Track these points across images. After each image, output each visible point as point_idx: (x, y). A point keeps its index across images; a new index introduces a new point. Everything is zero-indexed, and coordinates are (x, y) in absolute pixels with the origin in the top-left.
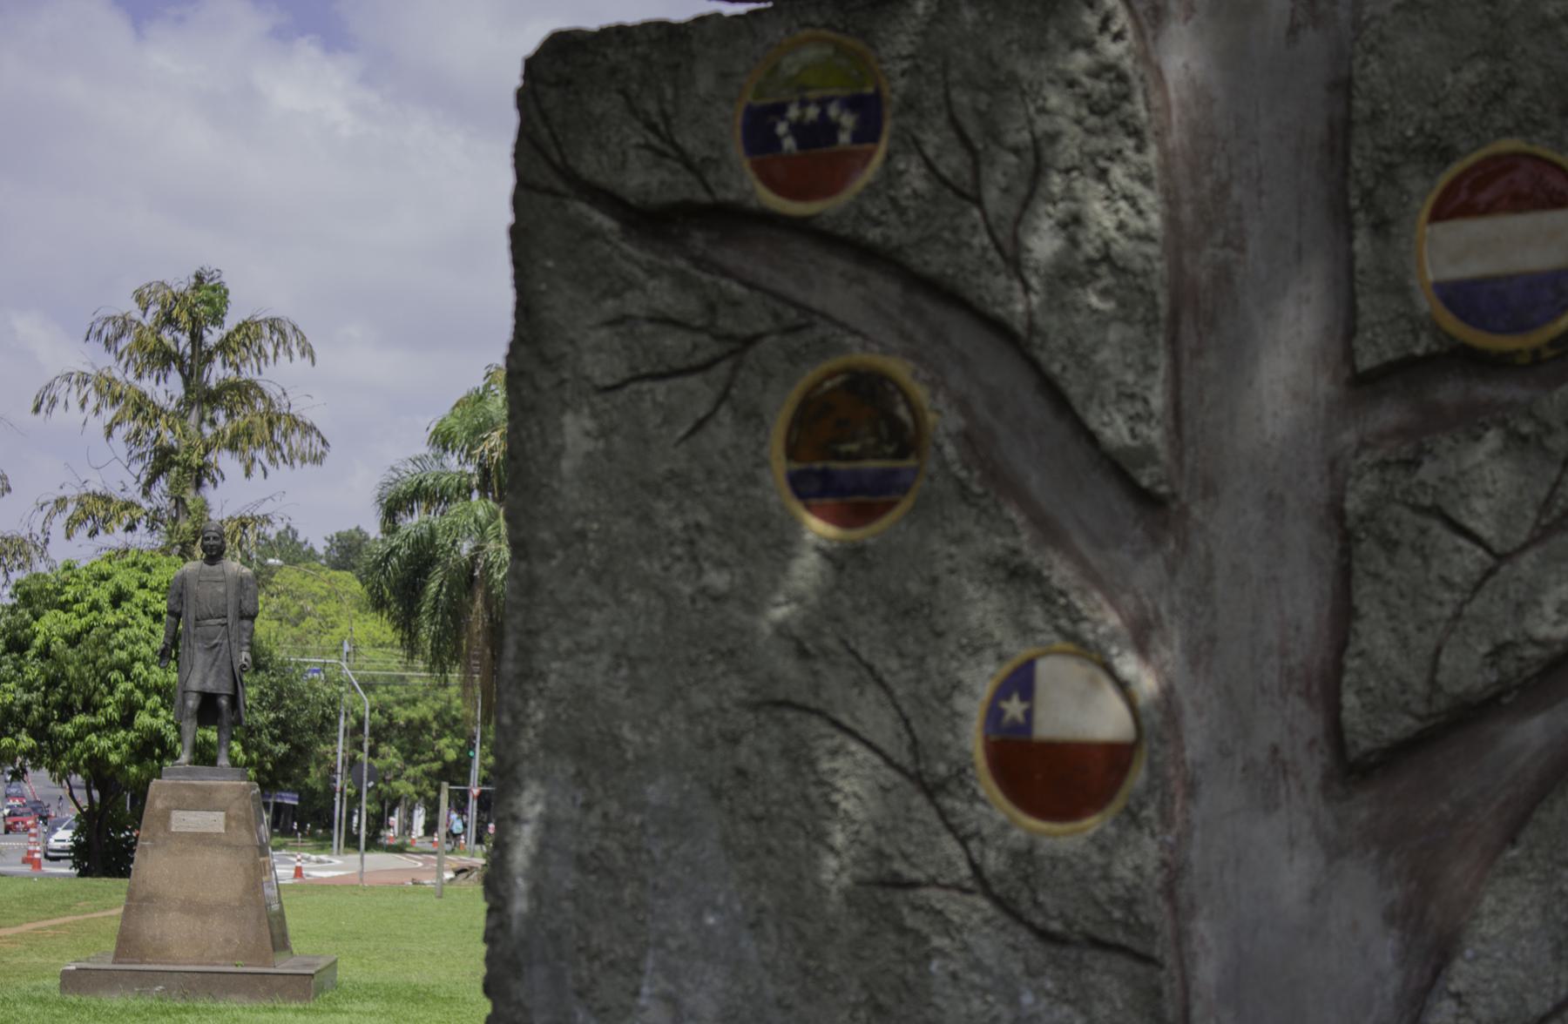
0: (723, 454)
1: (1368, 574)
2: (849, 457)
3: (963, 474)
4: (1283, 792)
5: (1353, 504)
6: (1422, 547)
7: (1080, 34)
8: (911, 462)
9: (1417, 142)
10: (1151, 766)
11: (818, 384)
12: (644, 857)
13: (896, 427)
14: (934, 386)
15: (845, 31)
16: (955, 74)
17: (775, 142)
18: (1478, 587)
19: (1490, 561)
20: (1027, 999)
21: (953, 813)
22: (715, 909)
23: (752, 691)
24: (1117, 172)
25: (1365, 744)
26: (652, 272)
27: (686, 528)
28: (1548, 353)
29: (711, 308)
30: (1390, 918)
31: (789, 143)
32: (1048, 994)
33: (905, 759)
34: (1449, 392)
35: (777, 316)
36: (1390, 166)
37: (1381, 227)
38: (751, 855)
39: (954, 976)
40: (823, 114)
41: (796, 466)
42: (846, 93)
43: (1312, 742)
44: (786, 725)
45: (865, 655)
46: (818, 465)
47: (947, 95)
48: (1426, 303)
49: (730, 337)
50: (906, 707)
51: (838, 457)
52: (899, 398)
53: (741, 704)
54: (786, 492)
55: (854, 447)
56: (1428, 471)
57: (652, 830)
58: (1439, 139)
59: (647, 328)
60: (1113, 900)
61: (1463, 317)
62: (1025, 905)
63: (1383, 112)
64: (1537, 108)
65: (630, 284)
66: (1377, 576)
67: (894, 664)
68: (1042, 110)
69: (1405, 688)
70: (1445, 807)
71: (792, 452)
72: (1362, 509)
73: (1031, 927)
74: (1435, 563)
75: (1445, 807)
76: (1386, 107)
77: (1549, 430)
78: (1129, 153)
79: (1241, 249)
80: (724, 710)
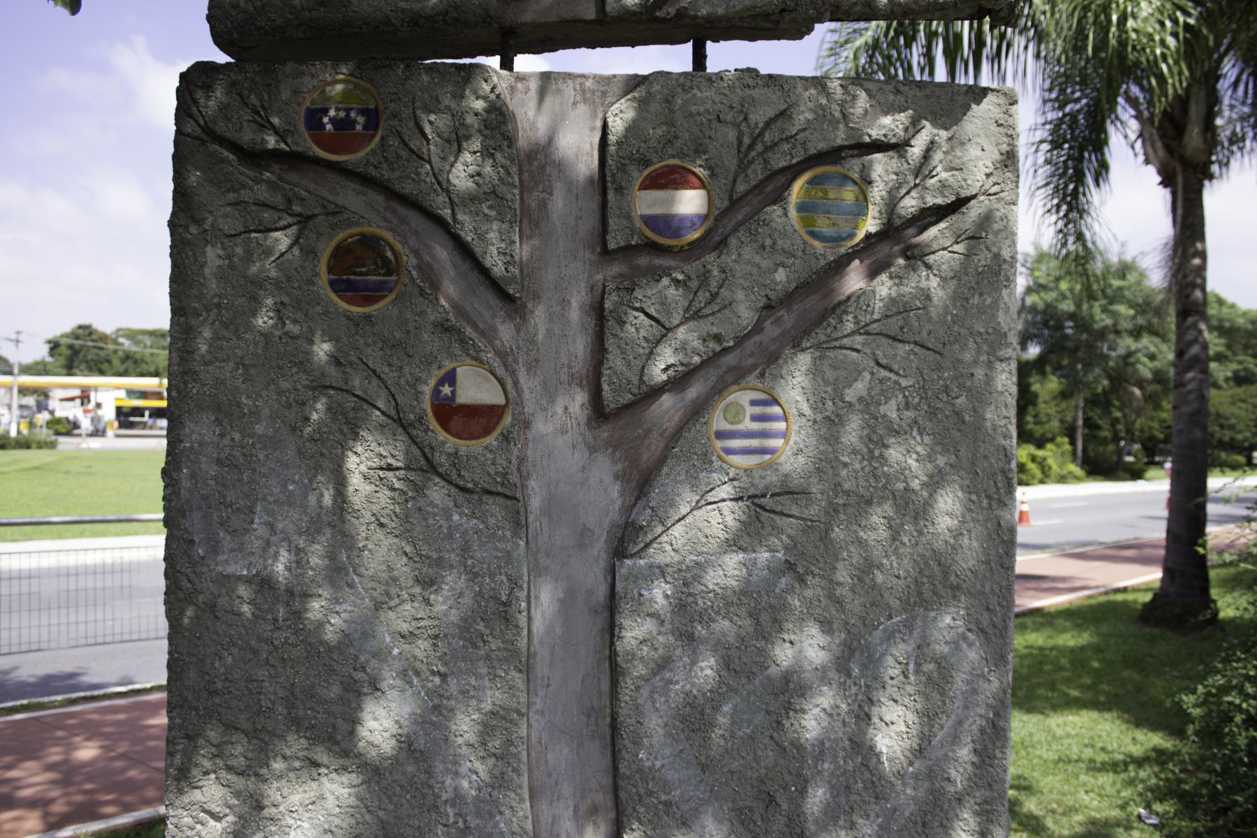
0: (296, 270)
2: (361, 274)
3: (422, 284)
5: (608, 305)
7: (481, 93)
8: (394, 278)
9: (636, 156)
10: (513, 415)
11: (346, 239)
12: (254, 458)
13: (386, 261)
14: (404, 244)
15: (361, 78)
16: (418, 104)
17: (323, 126)
20: (456, 517)
21: (417, 436)
22: (294, 482)
23: (312, 381)
24: (498, 156)
25: (612, 406)
26: (256, 182)
27: (275, 303)
28: (687, 248)
29: (289, 201)
30: (616, 477)
31: (329, 127)
32: (466, 515)
33: (393, 413)
34: (643, 260)
35: (324, 207)
36: (624, 165)
37: (619, 190)
38: (312, 457)
39: (420, 509)
40: (348, 115)
41: (332, 277)
42: (360, 107)
43: (583, 405)
45: (371, 365)
46: (345, 277)
47: (414, 113)
48: (639, 224)
49: (299, 215)
50: (392, 389)
51: (355, 274)
52: (387, 248)
53: (307, 387)
54: (328, 289)
55: (364, 270)
56: (638, 293)
57: (258, 446)
59: (254, 208)
60: (497, 473)
61: (653, 230)
62: (454, 476)
65: (244, 187)
66: (616, 336)
67: (387, 370)
68: (462, 124)
69: (629, 382)
70: (640, 431)
71: (330, 271)
72: (611, 307)
73: (457, 486)
77: (690, 278)
78: (505, 148)
79: (551, 194)
80: (296, 389)
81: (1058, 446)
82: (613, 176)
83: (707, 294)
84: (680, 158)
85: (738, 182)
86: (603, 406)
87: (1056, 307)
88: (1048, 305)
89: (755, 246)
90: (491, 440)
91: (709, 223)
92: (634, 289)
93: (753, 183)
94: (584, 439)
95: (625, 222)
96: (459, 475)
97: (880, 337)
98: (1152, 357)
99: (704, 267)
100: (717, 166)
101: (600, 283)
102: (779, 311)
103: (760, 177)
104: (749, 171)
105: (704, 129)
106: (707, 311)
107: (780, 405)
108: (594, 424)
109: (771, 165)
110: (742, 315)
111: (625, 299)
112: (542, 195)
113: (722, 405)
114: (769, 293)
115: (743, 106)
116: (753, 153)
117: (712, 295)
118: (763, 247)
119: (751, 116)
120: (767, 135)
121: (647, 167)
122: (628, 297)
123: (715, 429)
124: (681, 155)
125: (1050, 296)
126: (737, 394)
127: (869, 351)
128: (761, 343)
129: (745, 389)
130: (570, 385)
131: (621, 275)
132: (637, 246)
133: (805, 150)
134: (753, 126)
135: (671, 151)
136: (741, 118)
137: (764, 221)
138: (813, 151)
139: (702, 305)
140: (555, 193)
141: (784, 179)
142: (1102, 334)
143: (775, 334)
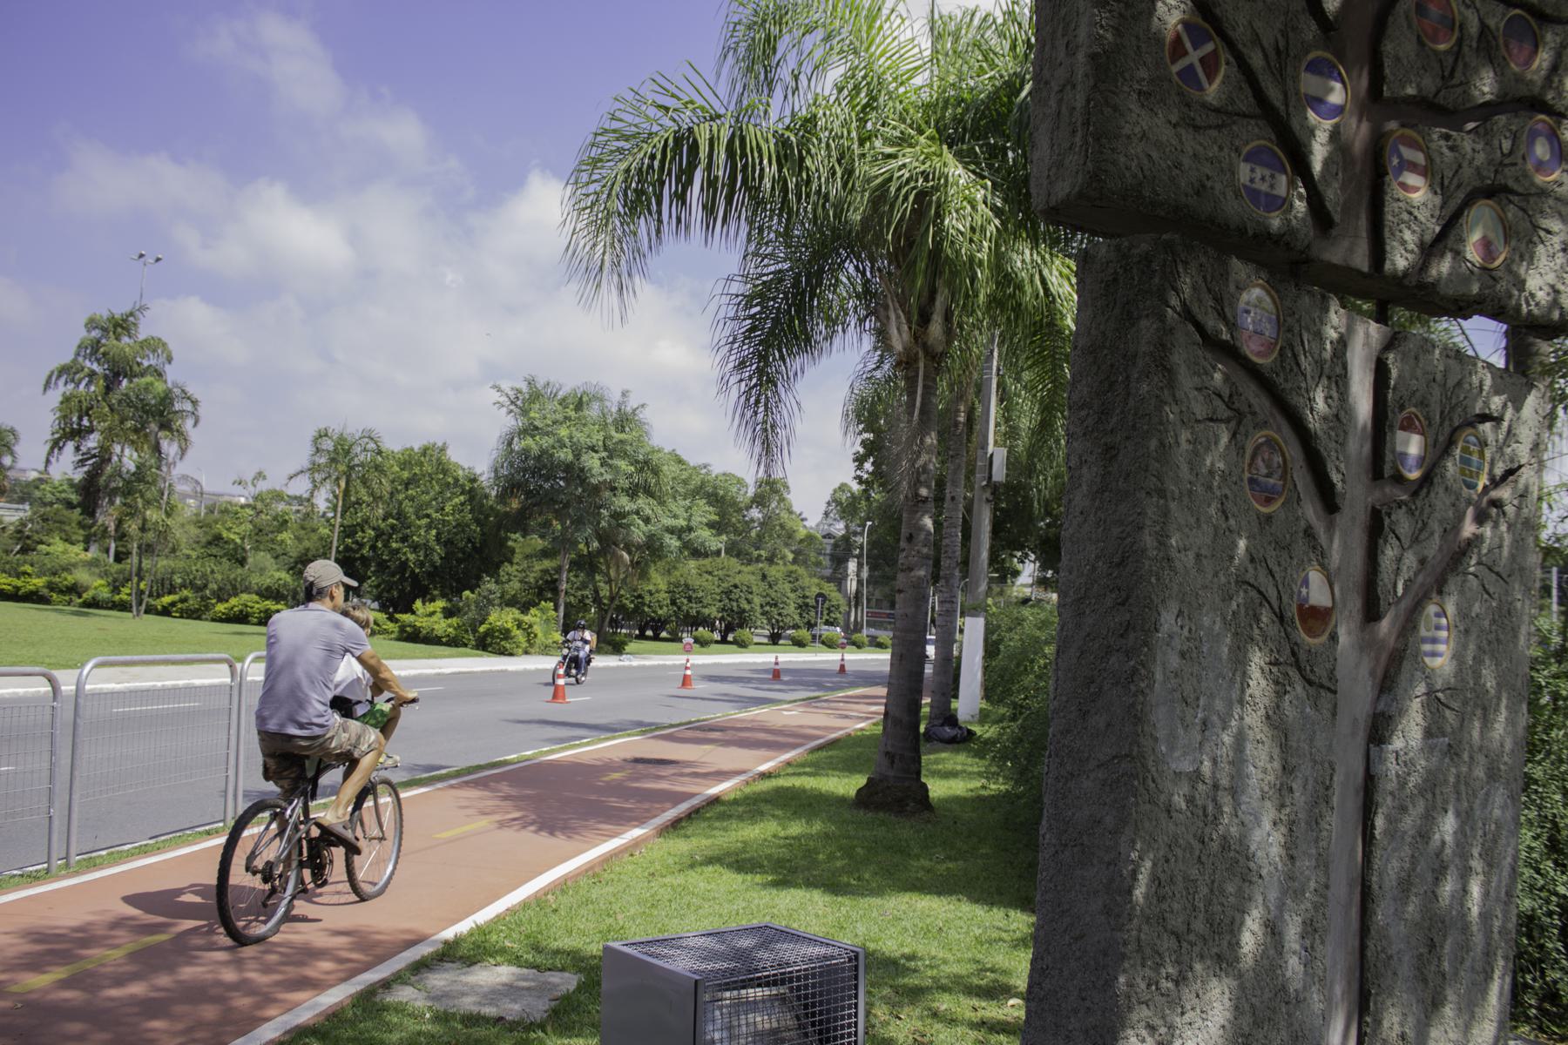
44: (1246, 592)
81: (543, 611)
87: (552, 455)
88: (543, 452)
90: (1324, 638)
96: (1312, 671)
98: (647, 520)
125: (546, 442)
142: (596, 490)
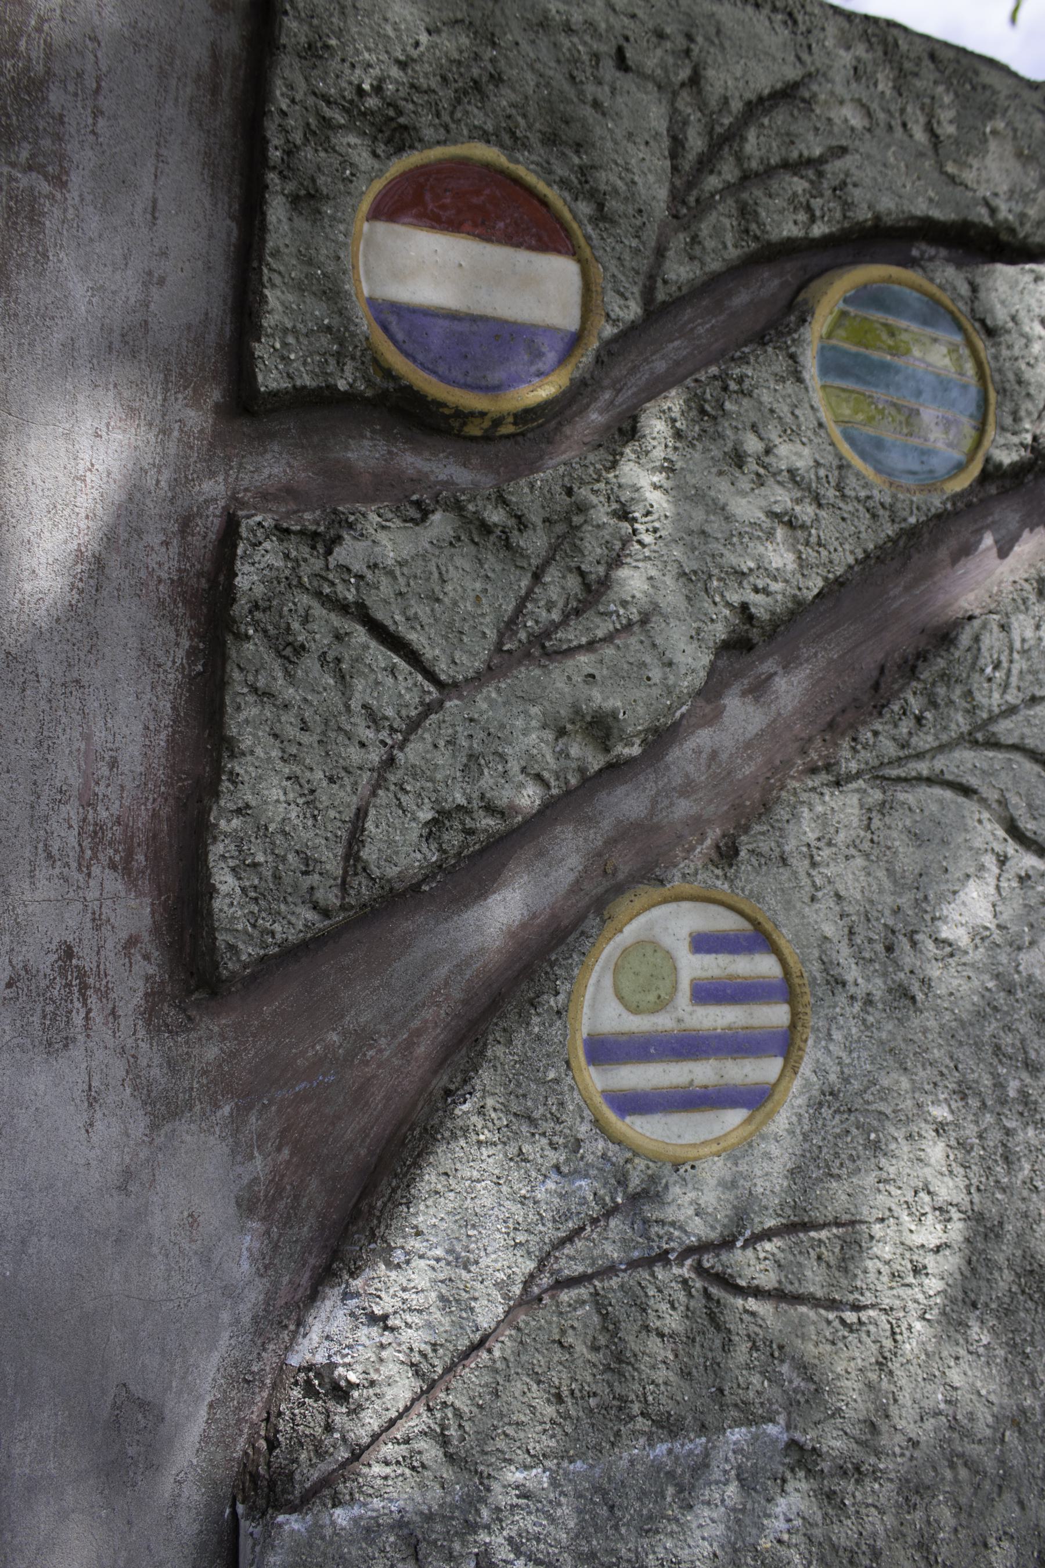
1: (254, 690)
4: (78, 1020)
6: (338, 660)
9: (372, 102)
18: (414, 725)
19: (435, 693)
25: (249, 951)
28: (508, 429)
36: (326, 123)
43: (132, 941)
58: (400, 113)
63: (327, 47)
64: (522, 122)
66: (264, 695)
69: (309, 864)
70: (334, 1037)
72: (259, 590)
74: (359, 684)
75: (334, 1037)
76: (333, 42)
77: (522, 523)
79: (60, 182)
82: (291, 151)
83: (573, 582)
84: (502, 146)
85: (670, 254)
86: (213, 949)
89: (716, 453)
91: (585, 357)
92: (338, 539)
93: (715, 265)
94: (132, 1068)
95: (319, 310)
97: (1017, 757)
99: (569, 492)
100: (616, 191)
101: (215, 510)
102: (762, 659)
103: (733, 253)
104: (705, 228)
105: (580, 76)
106: (573, 635)
107: (775, 950)
108: (170, 1013)
109: (761, 225)
110: (679, 658)
111: (305, 571)
112: (24, 181)
113: (610, 950)
114: (752, 597)
115: (690, 37)
116: (713, 182)
117: (587, 586)
118: (738, 459)
119: (710, 73)
120: (751, 135)
121: (400, 150)
122: (318, 564)
123: (584, 1031)
124: (506, 137)
126: (657, 912)
127: (993, 796)
128: (714, 755)
129: (678, 898)
130: (84, 867)
131: (290, 492)
132: (350, 398)
133: (847, 206)
134: (713, 103)
135: (478, 118)
136: (684, 74)
137: (740, 380)
138: (863, 214)
139: (556, 616)
140: (75, 179)
141: (776, 282)
143: (753, 729)
